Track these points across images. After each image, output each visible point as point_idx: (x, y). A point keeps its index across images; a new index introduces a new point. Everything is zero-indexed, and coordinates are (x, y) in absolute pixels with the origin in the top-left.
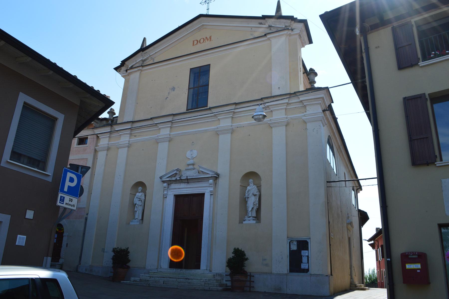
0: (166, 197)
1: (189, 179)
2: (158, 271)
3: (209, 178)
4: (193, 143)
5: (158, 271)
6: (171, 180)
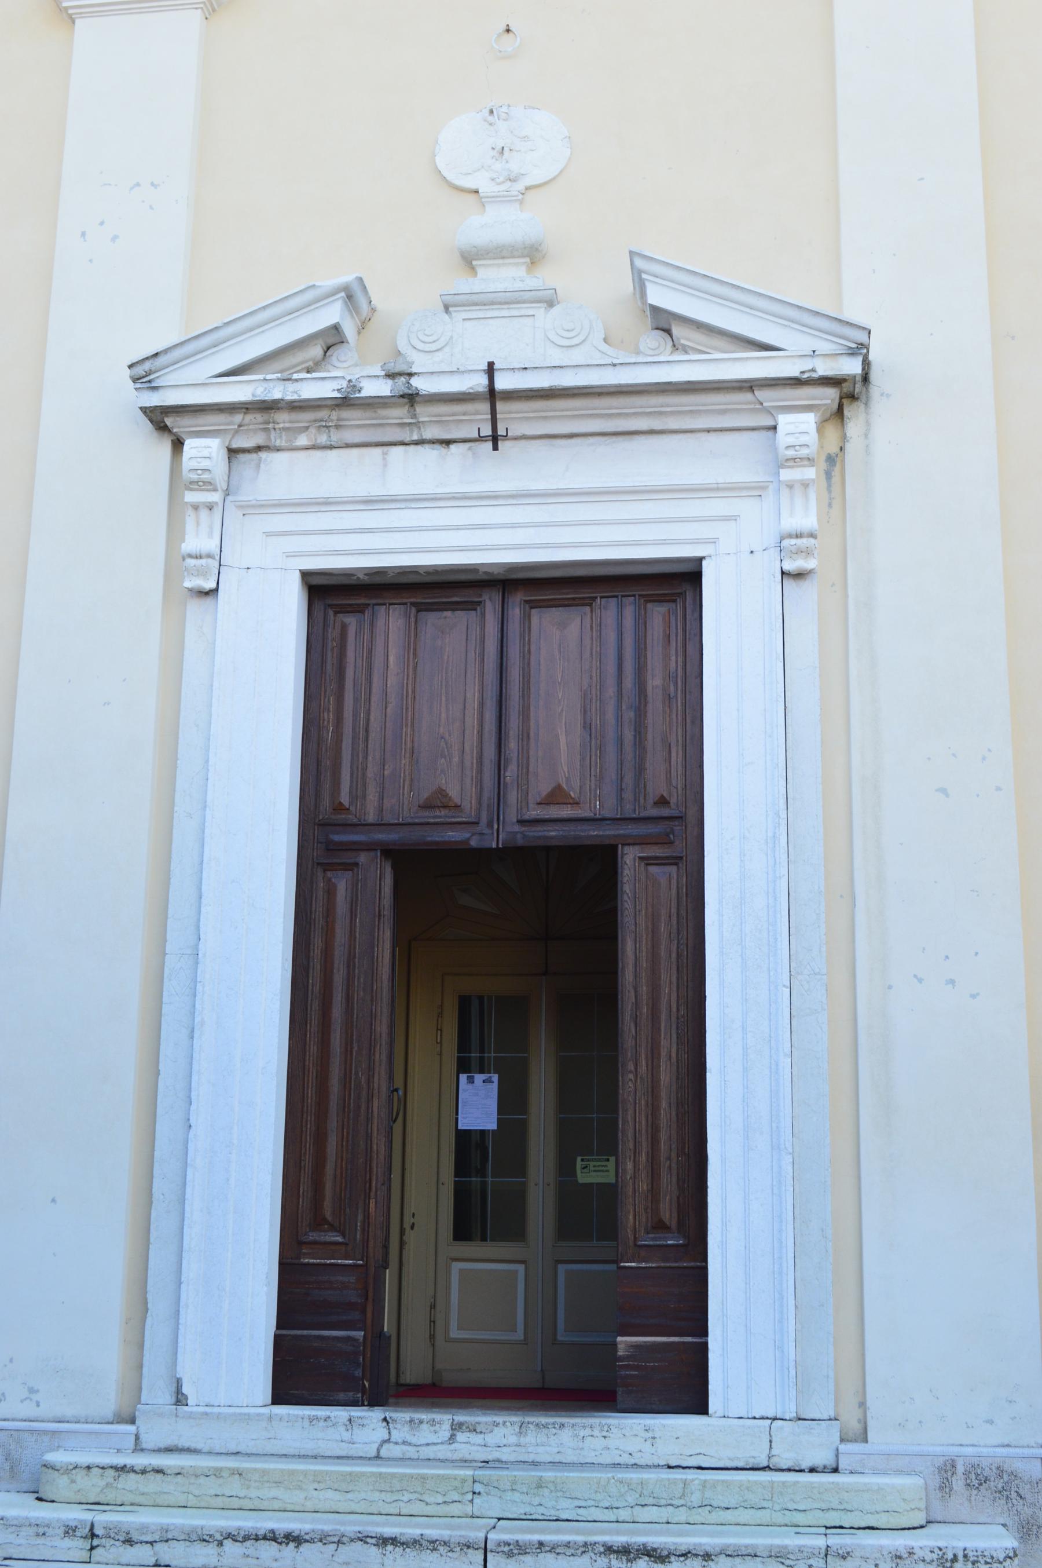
0: (213, 592)
1: (511, 395)
2: (138, 1448)
3: (761, 394)
4: (508, 43)
5: (148, 1441)
6: (277, 395)
